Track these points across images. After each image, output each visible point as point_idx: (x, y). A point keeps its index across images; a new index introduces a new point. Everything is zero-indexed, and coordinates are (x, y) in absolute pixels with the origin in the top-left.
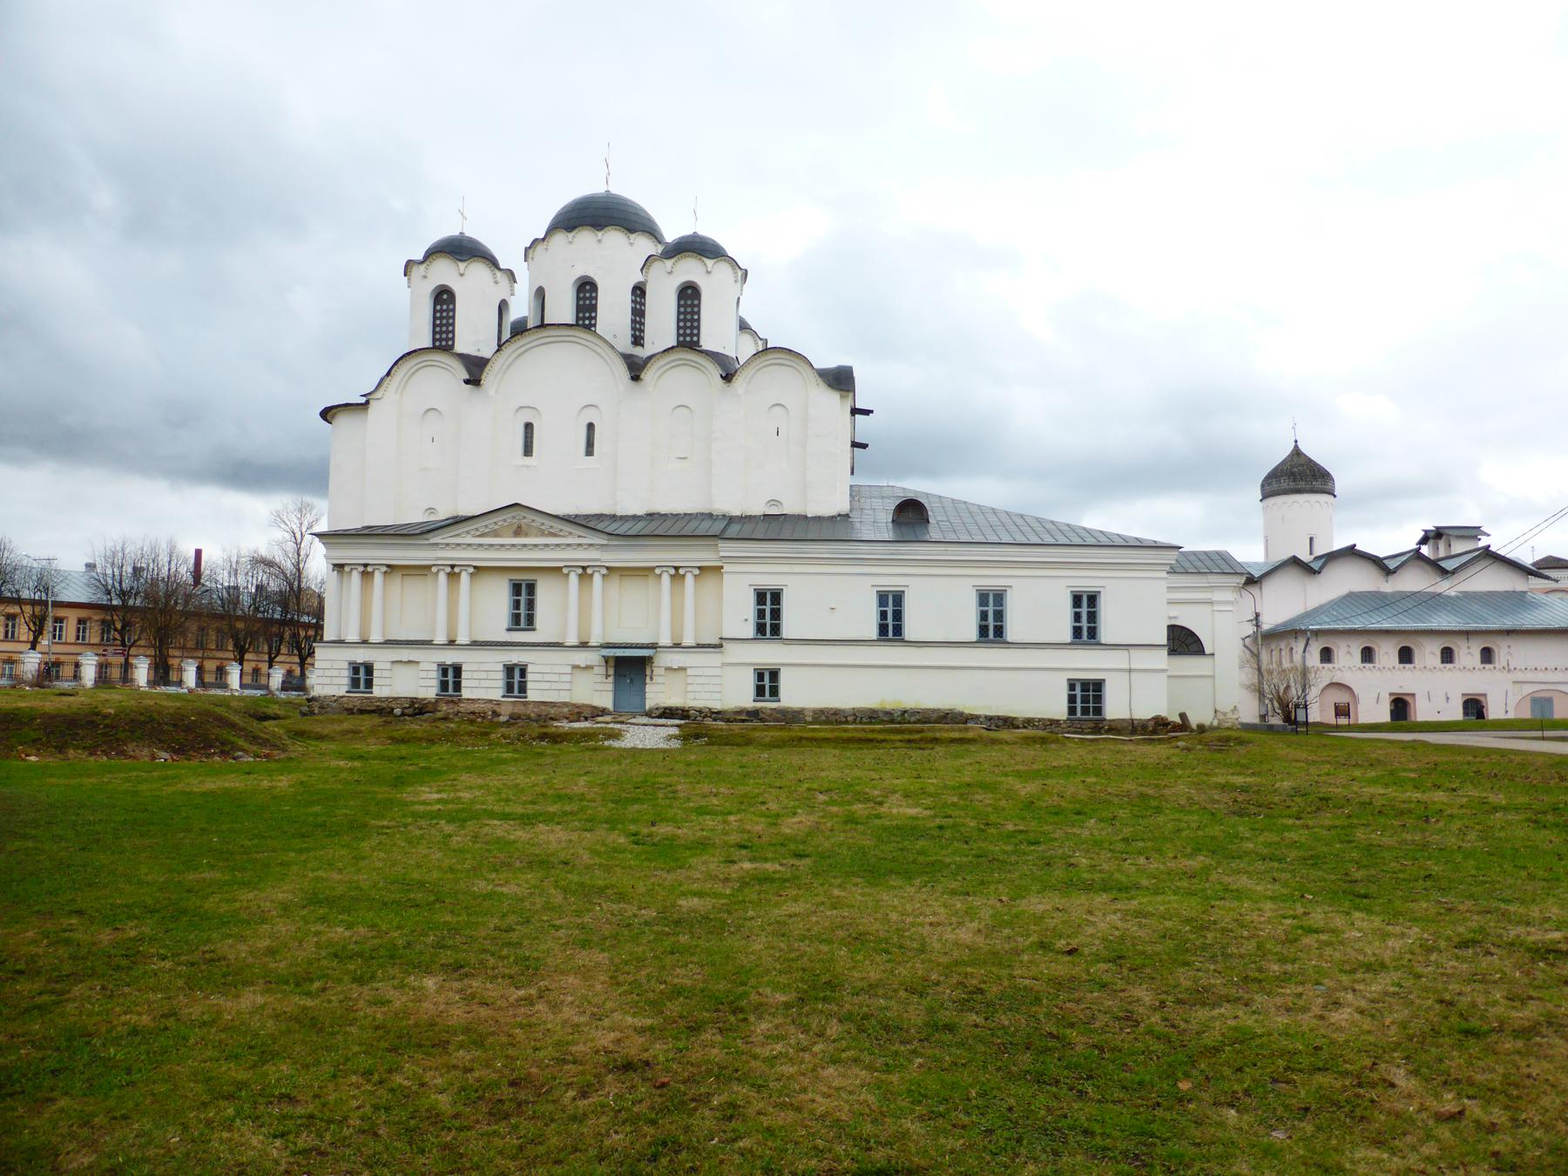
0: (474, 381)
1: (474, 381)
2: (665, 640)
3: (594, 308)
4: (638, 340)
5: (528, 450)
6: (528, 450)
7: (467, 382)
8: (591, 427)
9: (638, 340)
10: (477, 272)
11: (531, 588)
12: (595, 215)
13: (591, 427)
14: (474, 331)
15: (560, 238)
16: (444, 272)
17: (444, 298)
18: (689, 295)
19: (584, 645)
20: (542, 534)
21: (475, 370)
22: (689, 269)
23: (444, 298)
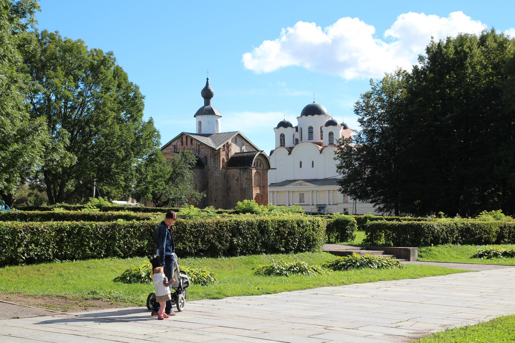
0: (290, 153)
1: (290, 153)
2: (327, 204)
3: (312, 132)
4: (322, 139)
5: (301, 167)
6: (301, 167)
7: (289, 154)
8: (313, 162)
9: (322, 139)
10: (289, 128)
11: (303, 194)
12: (312, 110)
13: (313, 162)
14: (289, 142)
15: (304, 117)
16: (282, 130)
17: (282, 136)
18: (331, 134)
19: (313, 205)
20: (305, 185)
21: (290, 150)
22: (331, 128)
23: (282, 136)
